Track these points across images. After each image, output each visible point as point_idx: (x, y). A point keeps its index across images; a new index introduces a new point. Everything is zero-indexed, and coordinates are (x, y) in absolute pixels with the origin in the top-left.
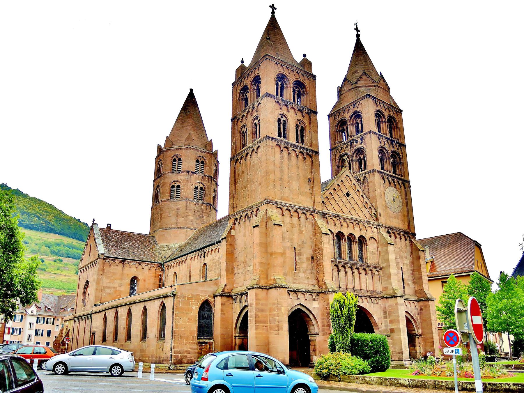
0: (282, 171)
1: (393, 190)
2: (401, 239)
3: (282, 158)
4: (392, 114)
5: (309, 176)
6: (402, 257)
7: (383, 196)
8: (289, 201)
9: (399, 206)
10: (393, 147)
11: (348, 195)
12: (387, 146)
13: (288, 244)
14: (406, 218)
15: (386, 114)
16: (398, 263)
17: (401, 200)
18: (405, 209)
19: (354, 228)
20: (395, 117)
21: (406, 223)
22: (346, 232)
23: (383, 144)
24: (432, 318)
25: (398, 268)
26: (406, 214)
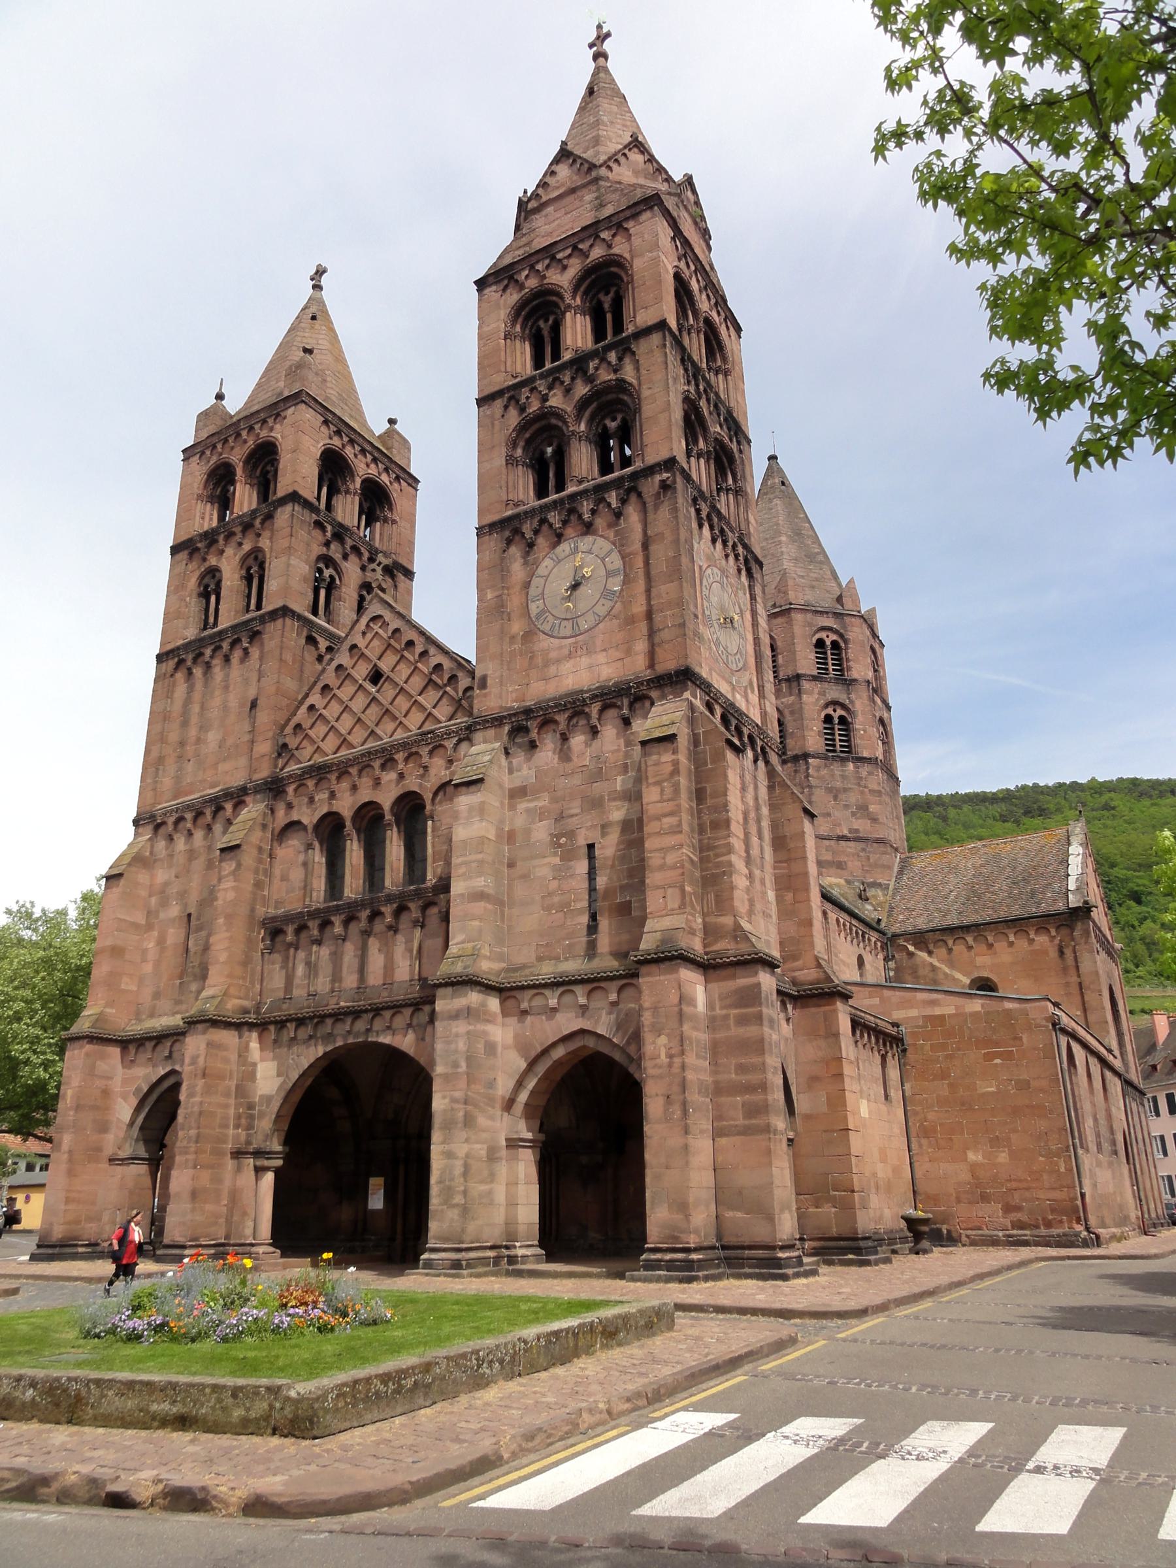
0: (185, 724)
1: (575, 551)
2: (594, 732)
3: (191, 689)
4: (597, 253)
5: (252, 693)
6: (595, 804)
7: (514, 602)
8: (191, 793)
9: (606, 593)
10: (590, 380)
11: (376, 677)
12: (556, 400)
13: (174, 911)
14: (643, 626)
15: (563, 279)
16: (571, 835)
17: (615, 561)
18: (640, 586)
19: (377, 782)
20: (616, 250)
21: (641, 646)
22: (346, 806)
23: (534, 406)
24: (648, 1049)
25: (568, 856)
26: (639, 608)
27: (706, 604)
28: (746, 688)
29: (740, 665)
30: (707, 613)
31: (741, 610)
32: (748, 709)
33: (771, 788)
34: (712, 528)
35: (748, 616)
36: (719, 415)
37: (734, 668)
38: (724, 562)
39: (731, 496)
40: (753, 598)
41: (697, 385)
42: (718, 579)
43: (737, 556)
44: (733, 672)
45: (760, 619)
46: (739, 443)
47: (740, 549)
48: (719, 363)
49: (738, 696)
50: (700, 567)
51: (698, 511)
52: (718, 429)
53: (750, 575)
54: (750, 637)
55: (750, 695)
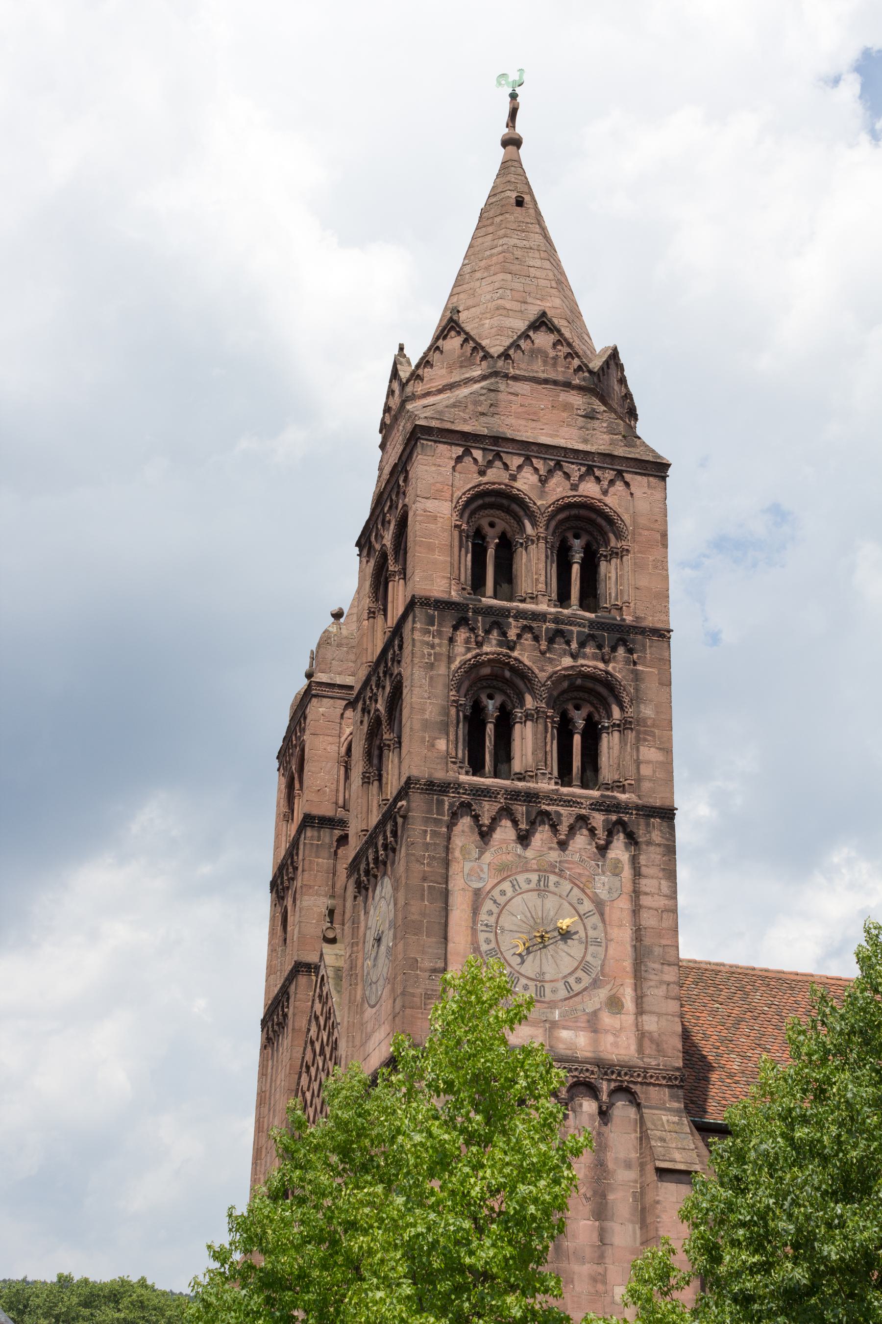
27: (482, 937)
28: (595, 1013)
29: (577, 988)
30: (484, 947)
31: (599, 906)
32: (595, 1042)
33: (641, 1139)
34: (515, 823)
35: (624, 904)
36: (568, 643)
37: (563, 993)
38: (554, 855)
39: (616, 735)
40: (637, 873)
41: (504, 634)
42: (533, 885)
43: (592, 831)
44: (552, 1005)
45: (645, 901)
46: (630, 651)
47: (598, 819)
48: (613, 542)
49: (565, 1034)
50: (477, 892)
51: (476, 818)
52: (567, 661)
53: (632, 839)
54: (623, 935)
55: (607, 1019)
